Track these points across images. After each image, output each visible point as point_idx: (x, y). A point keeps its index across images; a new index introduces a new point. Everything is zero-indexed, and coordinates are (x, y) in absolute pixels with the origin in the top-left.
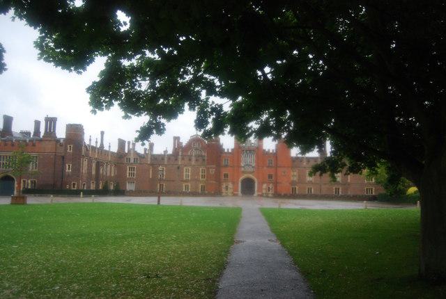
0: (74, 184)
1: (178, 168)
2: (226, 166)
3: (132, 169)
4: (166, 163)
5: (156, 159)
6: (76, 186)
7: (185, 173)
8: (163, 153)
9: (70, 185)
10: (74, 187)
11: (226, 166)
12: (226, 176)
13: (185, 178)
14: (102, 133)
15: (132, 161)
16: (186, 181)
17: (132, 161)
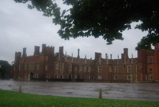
0: (49, 76)
1: (125, 66)
2: (151, 64)
3: (100, 68)
4: (118, 64)
5: (113, 62)
6: (50, 77)
7: (128, 69)
8: (93, 58)
9: (47, 77)
10: (49, 77)
11: (151, 64)
12: (151, 70)
13: (128, 72)
14: (79, 50)
15: (100, 63)
16: (129, 74)
17: (100, 63)
